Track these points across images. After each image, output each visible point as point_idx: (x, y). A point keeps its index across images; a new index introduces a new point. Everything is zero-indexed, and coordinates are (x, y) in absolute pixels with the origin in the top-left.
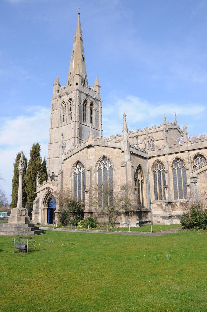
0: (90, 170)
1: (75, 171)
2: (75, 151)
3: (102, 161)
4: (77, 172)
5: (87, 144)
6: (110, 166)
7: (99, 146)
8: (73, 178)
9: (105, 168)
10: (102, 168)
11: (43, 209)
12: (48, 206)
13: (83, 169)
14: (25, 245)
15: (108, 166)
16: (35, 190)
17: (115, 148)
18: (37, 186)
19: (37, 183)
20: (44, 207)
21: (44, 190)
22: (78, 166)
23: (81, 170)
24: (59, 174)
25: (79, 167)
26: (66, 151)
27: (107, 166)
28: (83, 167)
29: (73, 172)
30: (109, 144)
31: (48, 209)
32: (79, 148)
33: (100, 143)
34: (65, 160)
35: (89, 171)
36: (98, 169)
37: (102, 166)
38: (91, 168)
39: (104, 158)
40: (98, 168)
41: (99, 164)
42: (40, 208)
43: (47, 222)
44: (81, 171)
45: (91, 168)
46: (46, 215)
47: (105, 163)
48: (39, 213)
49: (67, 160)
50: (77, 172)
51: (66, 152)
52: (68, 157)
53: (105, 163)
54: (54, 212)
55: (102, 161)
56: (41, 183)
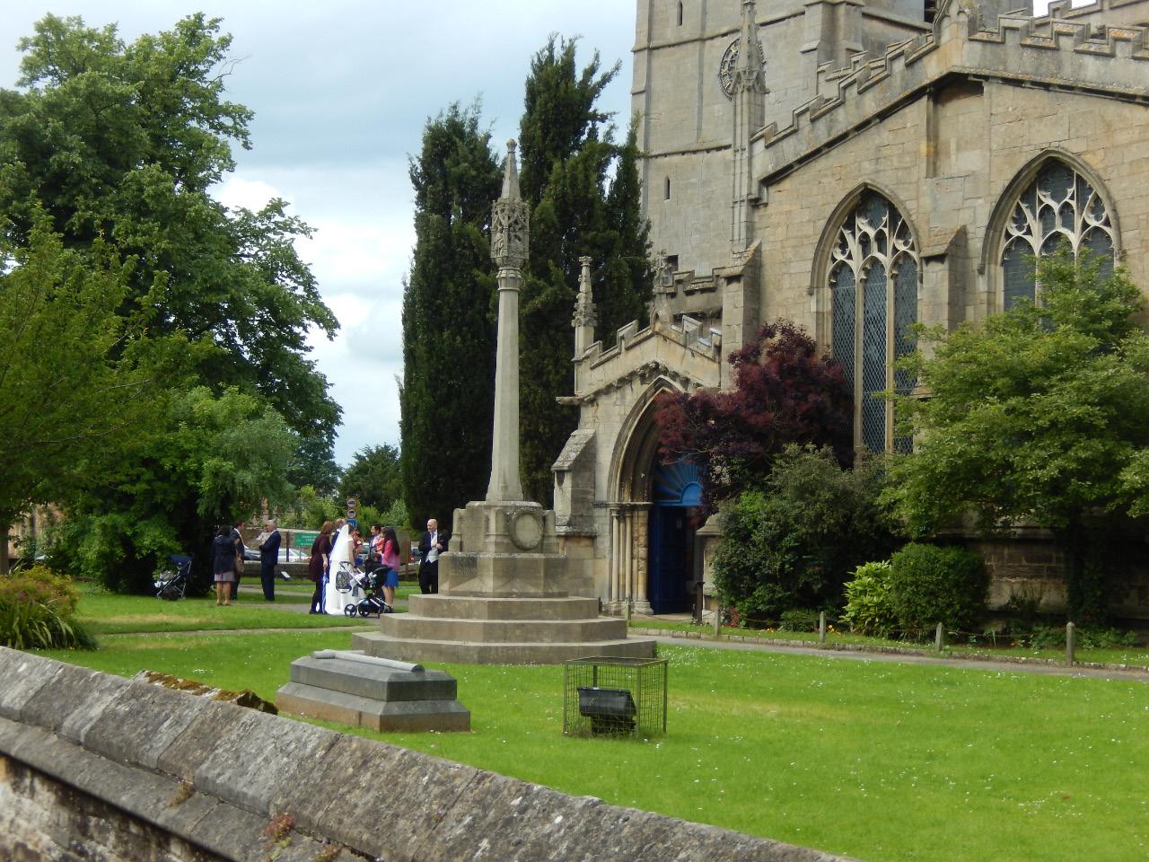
0: (954, 255)
1: (840, 257)
2: (845, 119)
3: (1039, 194)
4: (856, 264)
5: (932, 70)
6: (1093, 223)
7: (1017, 83)
8: (828, 307)
9: (1058, 236)
10: (1036, 242)
11: (623, 513)
12: (657, 493)
13: (902, 248)
14: (623, 699)
15: (1078, 223)
16: (568, 385)
17: (1129, 99)
18: (579, 355)
19: (582, 337)
20: (627, 501)
21: (628, 390)
22: (862, 224)
23: (882, 249)
24: (731, 279)
25: (872, 233)
26: (778, 112)
27: (1068, 224)
28: (903, 233)
29: (830, 266)
30: (1092, 70)
31: (652, 512)
32: (869, 96)
33: (1018, 62)
34: (771, 180)
35: (939, 258)
36: (1004, 244)
37: (1036, 226)
38: (961, 236)
39: (1051, 170)
40: (1008, 235)
41: (1012, 213)
42: (604, 505)
43: (650, 595)
44: (886, 260)
45: (961, 236)
46: (642, 552)
47: (1056, 207)
48: (592, 538)
49: (786, 185)
50: (856, 264)
51: (784, 124)
52: (792, 159)
53: (1056, 207)
54: (700, 531)
55: (1039, 194)
56: (605, 337)
